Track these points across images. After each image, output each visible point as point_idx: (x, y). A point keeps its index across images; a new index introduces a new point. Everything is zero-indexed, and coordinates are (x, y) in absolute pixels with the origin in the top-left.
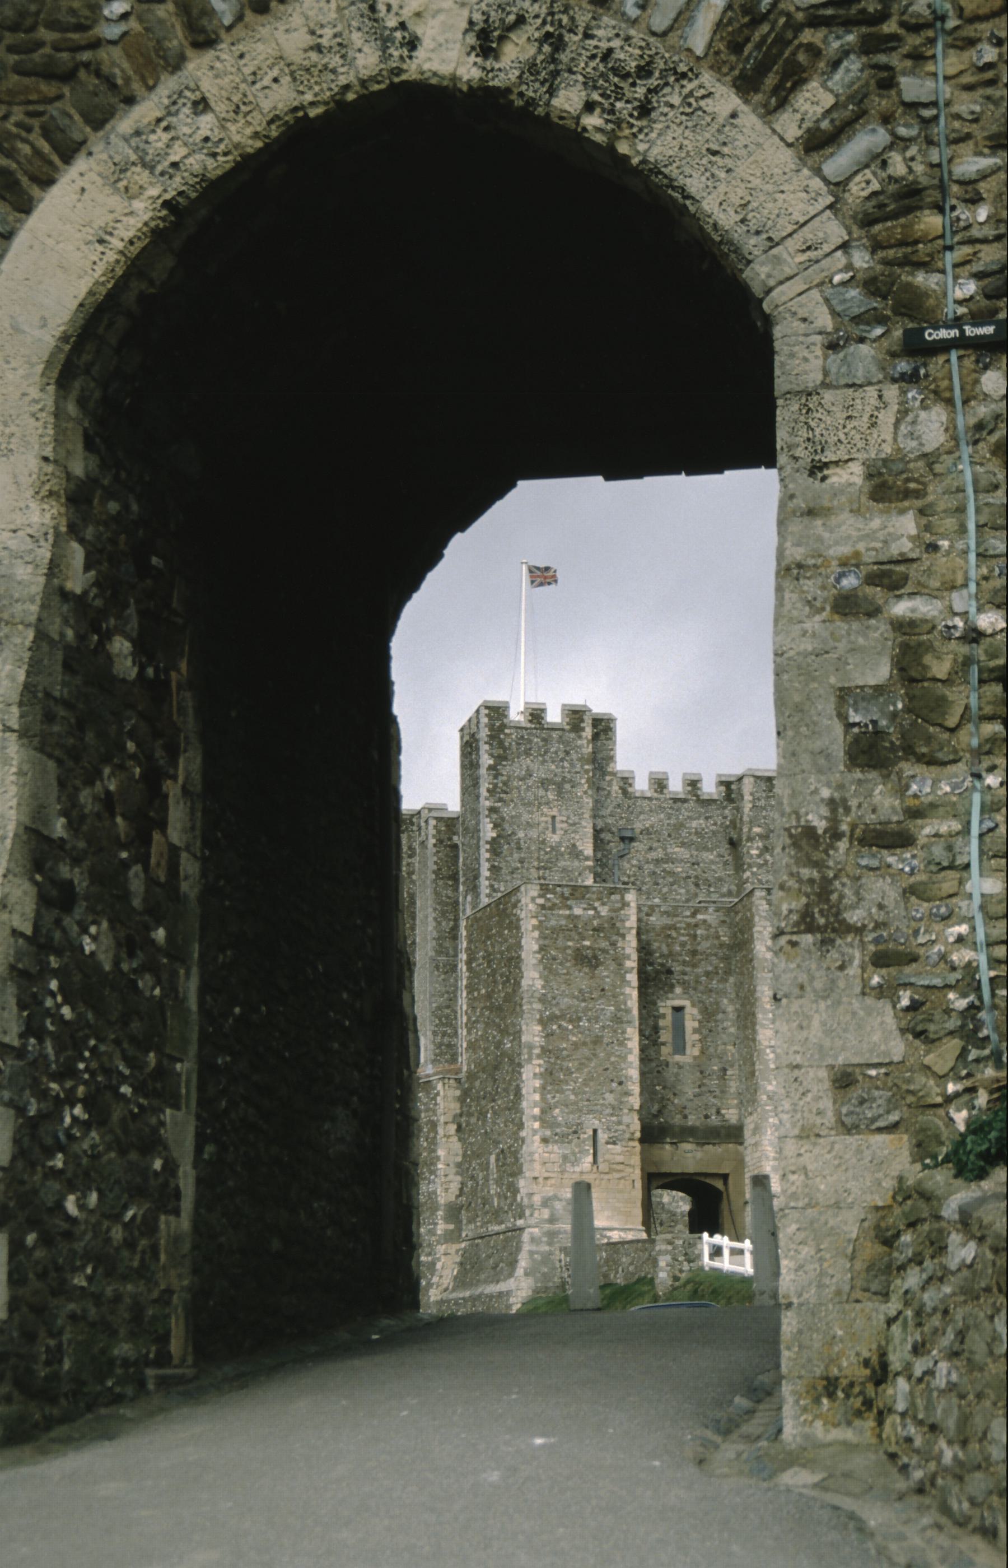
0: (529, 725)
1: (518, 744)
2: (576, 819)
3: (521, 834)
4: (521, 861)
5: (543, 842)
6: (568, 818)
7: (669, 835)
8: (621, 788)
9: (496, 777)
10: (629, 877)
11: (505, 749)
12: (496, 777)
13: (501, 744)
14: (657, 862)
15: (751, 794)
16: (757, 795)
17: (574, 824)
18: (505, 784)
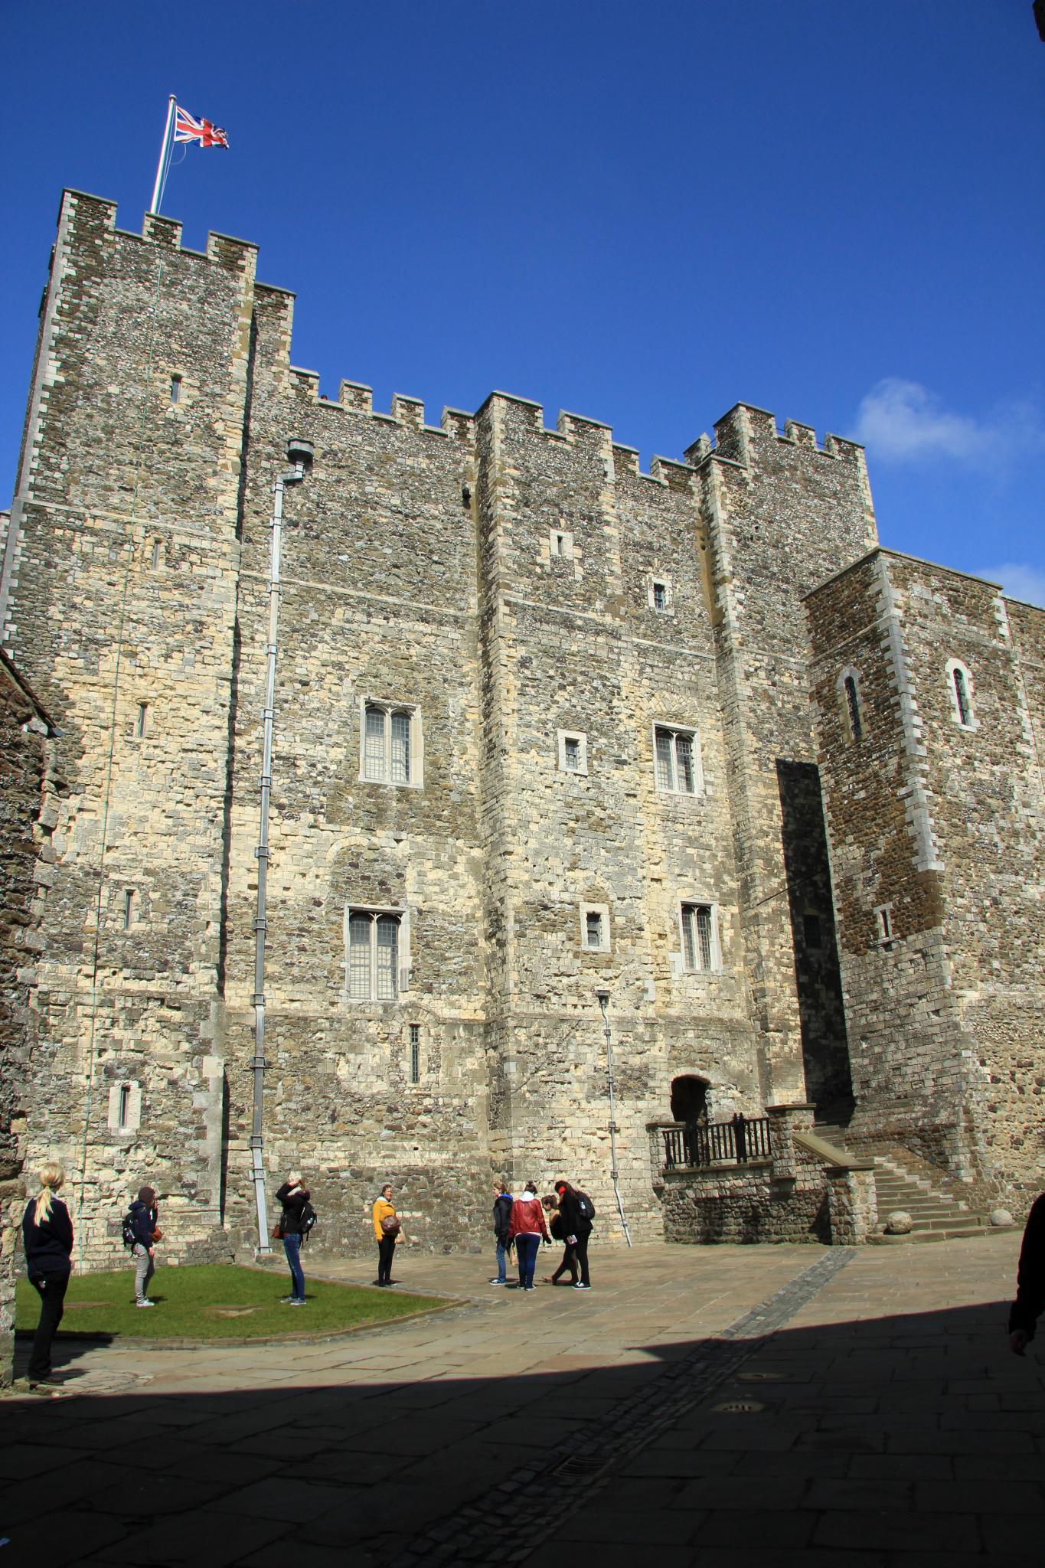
0: (149, 240)
1: (124, 259)
2: (217, 390)
3: (114, 389)
4: (109, 431)
5: (155, 409)
6: (203, 382)
7: (370, 469)
8: (293, 386)
9: (77, 295)
10: (299, 514)
11: (100, 261)
12: (77, 295)
13: (94, 252)
14: (350, 502)
15: (503, 421)
16: (512, 425)
17: (214, 395)
18: (94, 309)
